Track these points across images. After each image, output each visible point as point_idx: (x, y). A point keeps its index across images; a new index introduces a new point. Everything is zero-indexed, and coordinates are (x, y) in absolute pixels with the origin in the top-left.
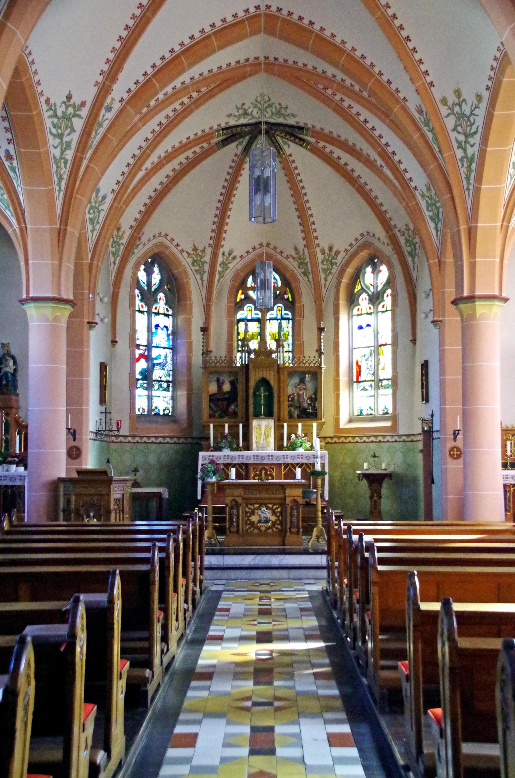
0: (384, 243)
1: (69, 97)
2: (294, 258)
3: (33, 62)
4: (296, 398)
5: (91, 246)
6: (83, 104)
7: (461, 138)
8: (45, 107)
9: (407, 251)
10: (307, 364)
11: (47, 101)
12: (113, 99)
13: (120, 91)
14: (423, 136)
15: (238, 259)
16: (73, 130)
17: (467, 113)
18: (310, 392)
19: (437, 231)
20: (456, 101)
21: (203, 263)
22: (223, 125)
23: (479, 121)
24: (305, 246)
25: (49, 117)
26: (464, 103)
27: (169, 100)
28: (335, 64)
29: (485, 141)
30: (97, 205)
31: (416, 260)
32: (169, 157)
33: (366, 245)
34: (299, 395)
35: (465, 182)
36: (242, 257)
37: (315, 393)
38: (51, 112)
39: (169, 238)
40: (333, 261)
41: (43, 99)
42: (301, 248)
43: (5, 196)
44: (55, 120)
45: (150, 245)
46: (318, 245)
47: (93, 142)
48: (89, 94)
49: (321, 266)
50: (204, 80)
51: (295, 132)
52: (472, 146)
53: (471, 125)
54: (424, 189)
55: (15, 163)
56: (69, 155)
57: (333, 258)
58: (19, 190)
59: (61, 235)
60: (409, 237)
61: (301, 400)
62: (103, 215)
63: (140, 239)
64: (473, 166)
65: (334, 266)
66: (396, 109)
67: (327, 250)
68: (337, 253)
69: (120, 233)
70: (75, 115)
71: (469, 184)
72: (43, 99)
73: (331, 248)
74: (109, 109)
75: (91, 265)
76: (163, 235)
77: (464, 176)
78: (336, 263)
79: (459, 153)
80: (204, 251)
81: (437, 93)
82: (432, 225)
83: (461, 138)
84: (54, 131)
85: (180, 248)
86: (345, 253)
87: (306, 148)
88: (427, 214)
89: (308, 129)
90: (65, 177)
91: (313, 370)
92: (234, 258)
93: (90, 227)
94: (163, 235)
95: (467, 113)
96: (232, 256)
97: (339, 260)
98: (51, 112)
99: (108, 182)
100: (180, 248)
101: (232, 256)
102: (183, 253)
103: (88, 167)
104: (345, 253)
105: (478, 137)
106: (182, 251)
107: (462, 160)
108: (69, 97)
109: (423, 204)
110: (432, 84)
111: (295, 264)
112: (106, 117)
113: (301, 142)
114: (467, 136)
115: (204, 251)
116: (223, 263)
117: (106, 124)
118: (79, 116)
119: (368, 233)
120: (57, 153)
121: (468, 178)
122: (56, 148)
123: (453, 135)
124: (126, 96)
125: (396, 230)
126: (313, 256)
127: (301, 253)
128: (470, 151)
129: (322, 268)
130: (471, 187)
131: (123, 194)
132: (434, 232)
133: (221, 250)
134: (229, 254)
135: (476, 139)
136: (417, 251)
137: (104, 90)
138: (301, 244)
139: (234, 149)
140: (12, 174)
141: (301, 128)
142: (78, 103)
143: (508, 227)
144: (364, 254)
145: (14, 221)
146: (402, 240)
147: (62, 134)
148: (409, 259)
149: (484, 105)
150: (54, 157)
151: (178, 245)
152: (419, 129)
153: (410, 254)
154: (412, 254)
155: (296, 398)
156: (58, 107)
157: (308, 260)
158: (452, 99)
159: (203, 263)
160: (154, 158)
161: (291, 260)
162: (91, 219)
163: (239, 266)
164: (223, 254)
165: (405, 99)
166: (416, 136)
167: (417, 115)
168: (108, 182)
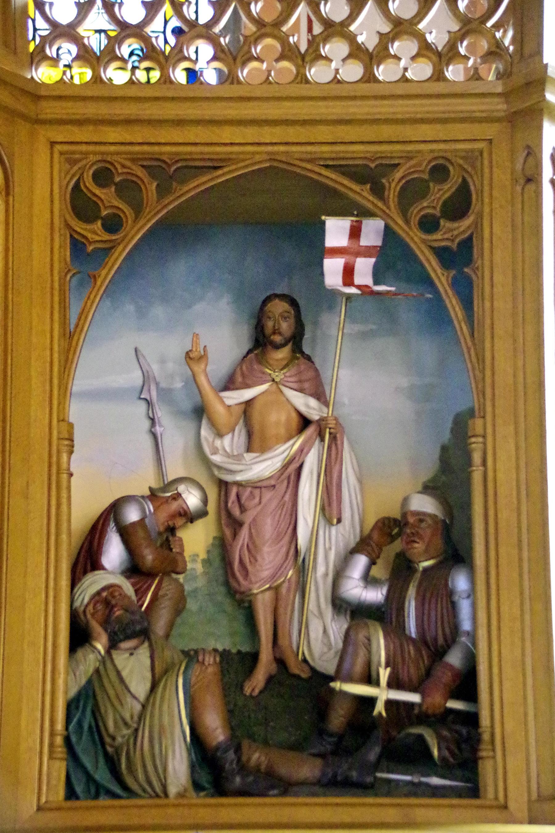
4: (196, 541)
10: (335, 65)
18: (386, 472)
34: (231, 503)
37: (451, 477)
61: (265, 568)
91: (427, 141)
155: (196, 541)
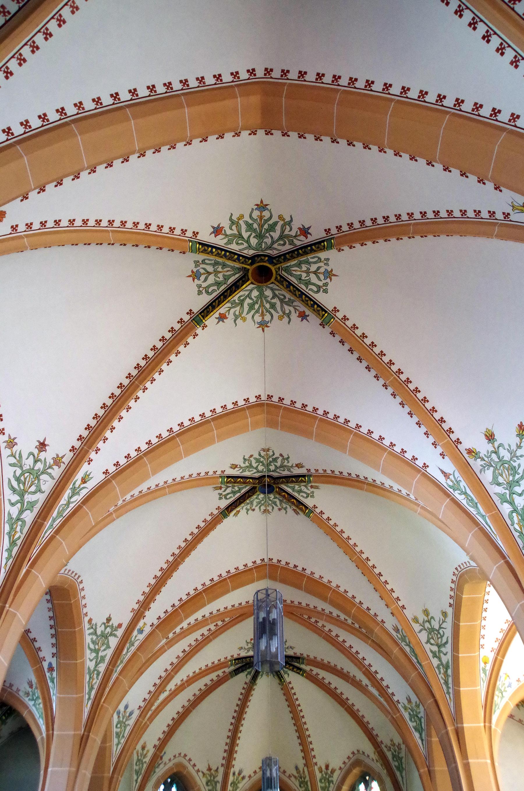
0: (373, 760)
1: (109, 620)
2: (295, 777)
3: (83, 589)
5: (114, 760)
6: (120, 626)
7: (435, 648)
9: (395, 766)
11: (90, 621)
12: (145, 624)
13: (152, 616)
14: (401, 649)
15: (247, 779)
16: (108, 647)
17: (437, 627)
19: (422, 740)
20: (426, 619)
21: (216, 783)
22: (236, 656)
23: (448, 632)
24: (305, 765)
26: (432, 620)
27: (192, 629)
28: (324, 599)
29: (456, 648)
30: (124, 720)
31: (404, 774)
32: (190, 681)
33: (357, 763)
35: (444, 686)
36: (250, 777)
38: (92, 631)
39: (187, 758)
40: (330, 779)
42: (301, 766)
43: (41, 706)
44: (94, 637)
45: (170, 764)
46: (316, 764)
47: (124, 658)
48: (125, 619)
49: (319, 784)
50: (220, 615)
51: (293, 662)
52: (445, 655)
53: (442, 637)
54: (406, 702)
55: (55, 674)
56: (102, 668)
57: (330, 776)
58: (54, 698)
59: (84, 740)
60: (395, 752)
62: (128, 729)
63: (161, 758)
64: (450, 672)
65: (331, 784)
66: (377, 630)
67: (324, 768)
68: (333, 771)
69: (145, 752)
70: (111, 634)
71: (448, 688)
73: (327, 767)
74: (141, 631)
75: (112, 777)
76: (182, 755)
77: (442, 681)
78: (332, 781)
79: (435, 662)
80: (217, 770)
81: (409, 614)
82: (417, 735)
83: (435, 648)
84: (92, 646)
85: (196, 768)
86: (340, 771)
87: (302, 675)
88: (411, 724)
89: (303, 659)
90: (96, 687)
92: (243, 778)
93: (116, 741)
94: (182, 755)
95: (437, 627)
96: (242, 776)
97: (336, 777)
98: (92, 631)
99: (136, 696)
100: (196, 768)
101: (242, 776)
102: (199, 773)
103: (117, 678)
104: (340, 771)
105: (449, 647)
106: (198, 771)
107: (438, 667)
108: (109, 620)
109: (406, 716)
110: (403, 607)
111: (297, 783)
112: (138, 638)
113: (299, 670)
114: (439, 646)
115: (217, 770)
116: (233, 783)
117: (137, 644)
118: (115, 636)
119: (358, 751)
120: (91, 665)
121: (446, 683)
122: (91, 660)
123: (428, 647)
124: (156, 622)
125: (383, 746)
126: (312, 774)
127: (302, 772)
128: (444, 659)
129: (321, 787)
130: (451, 691)
131: (149, 710)
132: (420, 741)
133: (232, 770)
134: (239, 774)
135: (448, 648)
136: (404, 766)
137: (138, 615)
138: (301, 763)
139: (243, 678)
140: (50, 684)
141: (298, 658)
142: (116, 624)
143: (490, 728)
144: (356, 771)
145: (43, 728)
146: (389, 755)
147: (99, 650)
148: (398, 774)
149: (450, 619)
150: (89, 668)
151: (194, 765)
152: (397, 644)
153: (398, 768)
154: (400, 768)
156: (98, 627)
157: (307, 778)
158: (422, 617)
159: (216, 783)
160: (177, 680)
161: (293, 779)
162: (117, 734)
163: (247, 786)
164: (234, 774)
165: (383, 621)
166: (396, 651)
167: (394, 633)
168: (136, 696)
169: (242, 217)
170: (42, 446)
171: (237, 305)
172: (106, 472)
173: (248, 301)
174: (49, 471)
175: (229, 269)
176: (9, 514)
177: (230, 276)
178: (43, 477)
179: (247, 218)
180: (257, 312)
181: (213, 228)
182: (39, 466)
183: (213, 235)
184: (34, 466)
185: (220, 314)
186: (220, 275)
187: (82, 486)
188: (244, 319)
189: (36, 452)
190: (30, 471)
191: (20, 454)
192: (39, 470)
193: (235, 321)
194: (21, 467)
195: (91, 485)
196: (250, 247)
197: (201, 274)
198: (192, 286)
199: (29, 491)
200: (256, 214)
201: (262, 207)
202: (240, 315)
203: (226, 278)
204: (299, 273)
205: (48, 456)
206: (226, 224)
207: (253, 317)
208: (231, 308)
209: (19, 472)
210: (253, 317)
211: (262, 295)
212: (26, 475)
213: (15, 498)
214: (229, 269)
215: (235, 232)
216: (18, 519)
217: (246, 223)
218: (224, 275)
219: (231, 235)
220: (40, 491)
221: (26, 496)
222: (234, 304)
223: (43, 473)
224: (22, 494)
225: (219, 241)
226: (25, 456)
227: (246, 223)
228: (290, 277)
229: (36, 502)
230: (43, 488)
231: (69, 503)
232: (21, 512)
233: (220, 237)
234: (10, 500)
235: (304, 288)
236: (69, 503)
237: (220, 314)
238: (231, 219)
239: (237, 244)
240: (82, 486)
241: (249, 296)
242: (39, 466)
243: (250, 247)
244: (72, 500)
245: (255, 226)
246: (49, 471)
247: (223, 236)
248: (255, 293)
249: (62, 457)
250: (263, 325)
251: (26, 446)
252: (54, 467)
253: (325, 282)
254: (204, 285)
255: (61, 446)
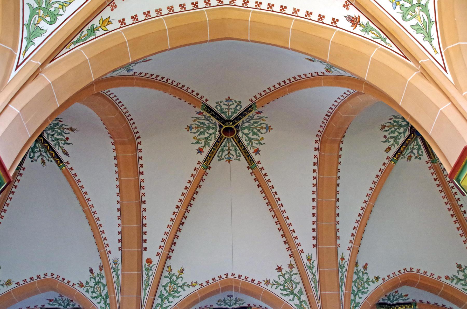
8: (448, 282)
25: (456, 283)
41: (443, 279)
72: (443, 279)
169: (195, 138)
170: (279, 269)
171: (251, 141)
172: (314, 246)
173: (250, 136)
174: (292, 273)
175: (227, 144)
176: (295, 304)
177: (232, 143)
178: (293, 278)
179: (196, 135)
180: (259, 131)
181: (198, 153)
182: (287, 276)
183: (202, 153)
184: (285, 278)
185: (254, 153)
186: (231, 148)
187: (311, 262)
188: (262, 138)
189: (280, 273)
190: (286, 282)
191: (275, 281)
192: (288, 277)
193: (261, 144)
194: (281, 285)
195: (314, 258)
196: (214, 133)
197: (229, 157)
198: (234, 163)
199: (293, 288)
200: (194, 130)
201: (189, 128)
202: (258, 140)
203: (233, 145)
204: (230, 113)
205: (286, 269)
206: (198, 146)
207: (262, 133)
208: (252, 146)
209: (282, 287)
210: (262, 133)
211: (248, 128)
212: (286, 285)
213: (291, 297)
214: (227, 144)
215: (203, 141)
216: (301, 302)
217: (199, 135)
218: (231, 146)
219: (205, 144)
220: (297, 284)
221: (295, 292)
222: (250, 144)
223: (291, 277)
224: (292, 292)
225: (207, 150)
226: (277, 280)
227: (199, 135)
228: (233, 117)
229: (301, 289)
230: (297, 281)
231: (314, 275)
232: (299, 299)
233: (204, 150)
234: (290, 300)
235: (238, 112)
236: (314, 275)
237: (254, 153)
238: (195, 144)
239: (211, 140)
240: (311, 262)
241: (247, 135)
242: (287, 276)
243: (214, 133)
244: (314, 272)
245: (202, 130)
246: (292, 273)
247: (205, 148)
248: (246, 131)
249: (291, 263)
250: (269, 129)
251: (274, 276)
252: (292, 270)
253: (234, 102)
254: (235, 157)
255: (285, 260)
